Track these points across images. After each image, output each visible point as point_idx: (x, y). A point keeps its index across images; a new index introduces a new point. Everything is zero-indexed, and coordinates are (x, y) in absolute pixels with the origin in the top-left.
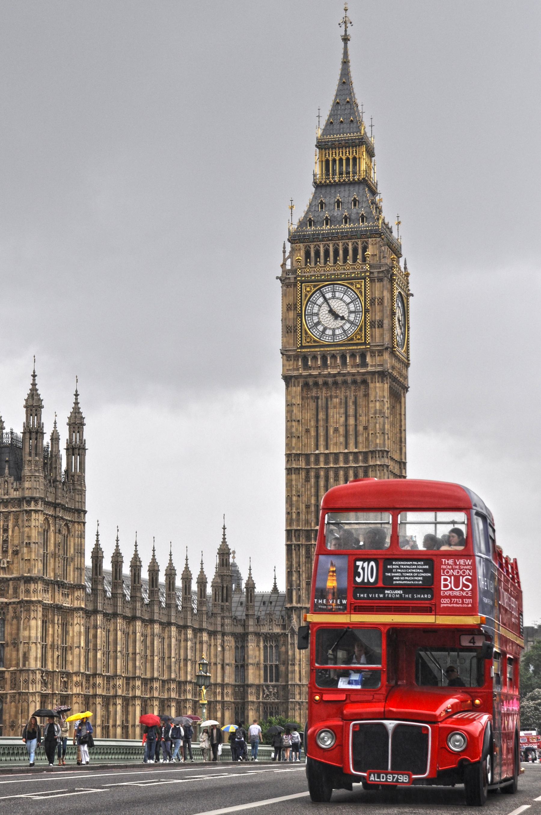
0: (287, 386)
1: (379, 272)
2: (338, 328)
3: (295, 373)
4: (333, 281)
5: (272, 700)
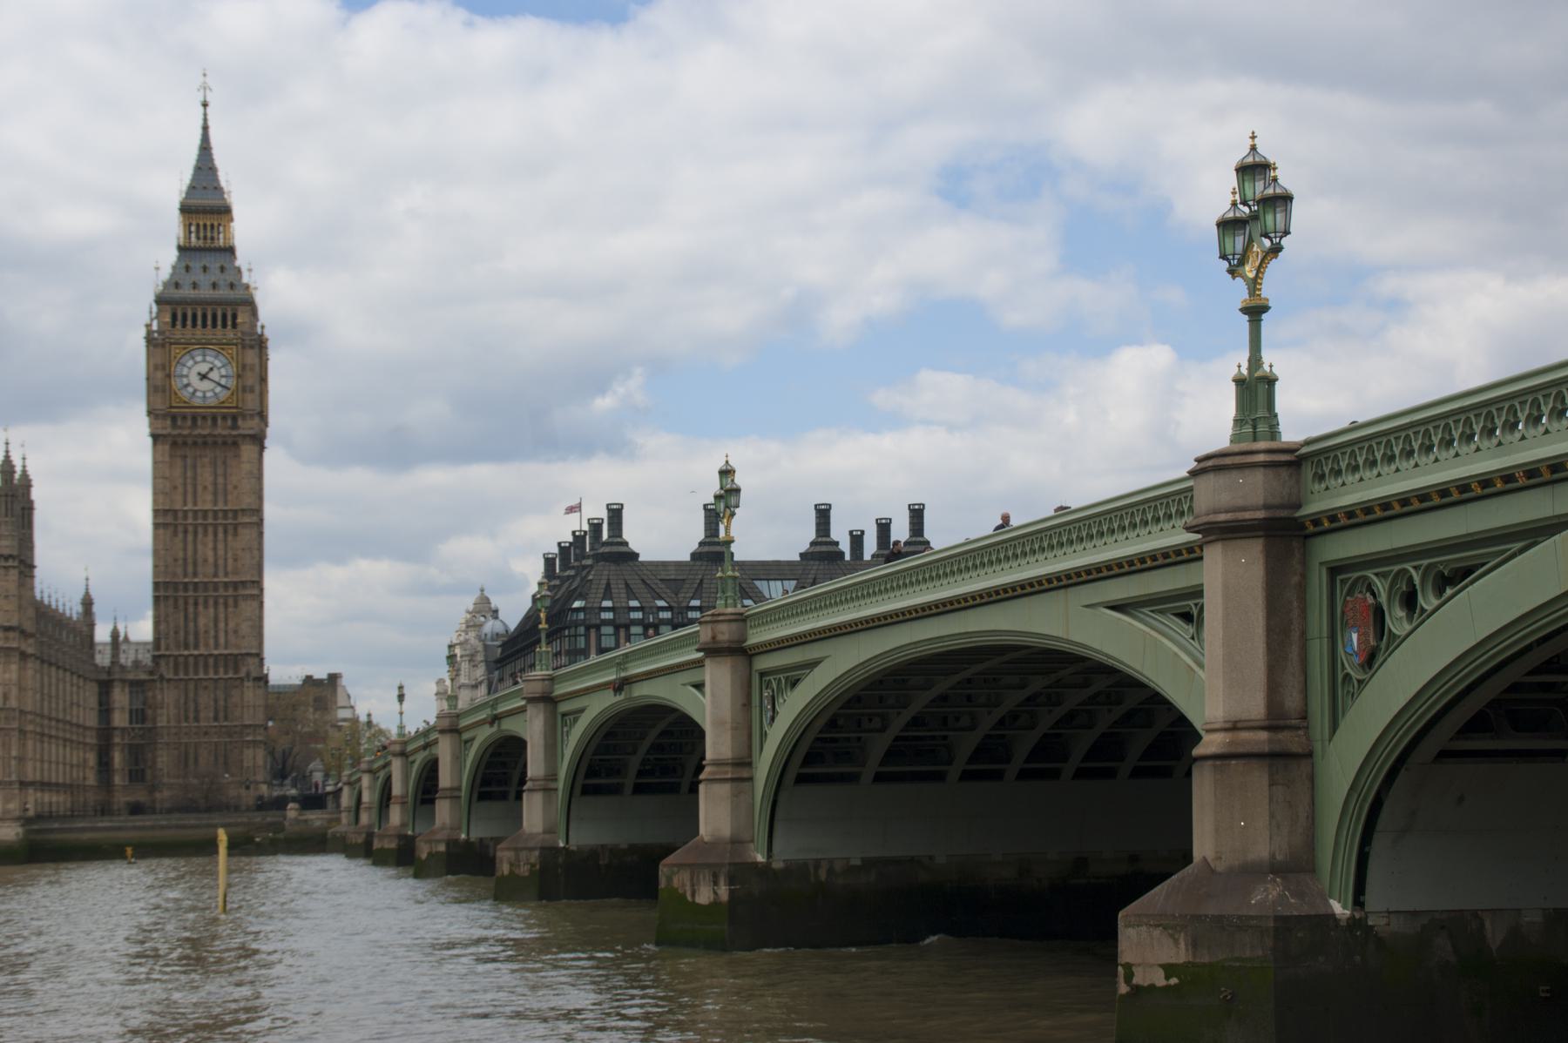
1: (251, 340)
2: (208, 391)
3: (164, 432)
4: (204, 345)
5: (136, 742)
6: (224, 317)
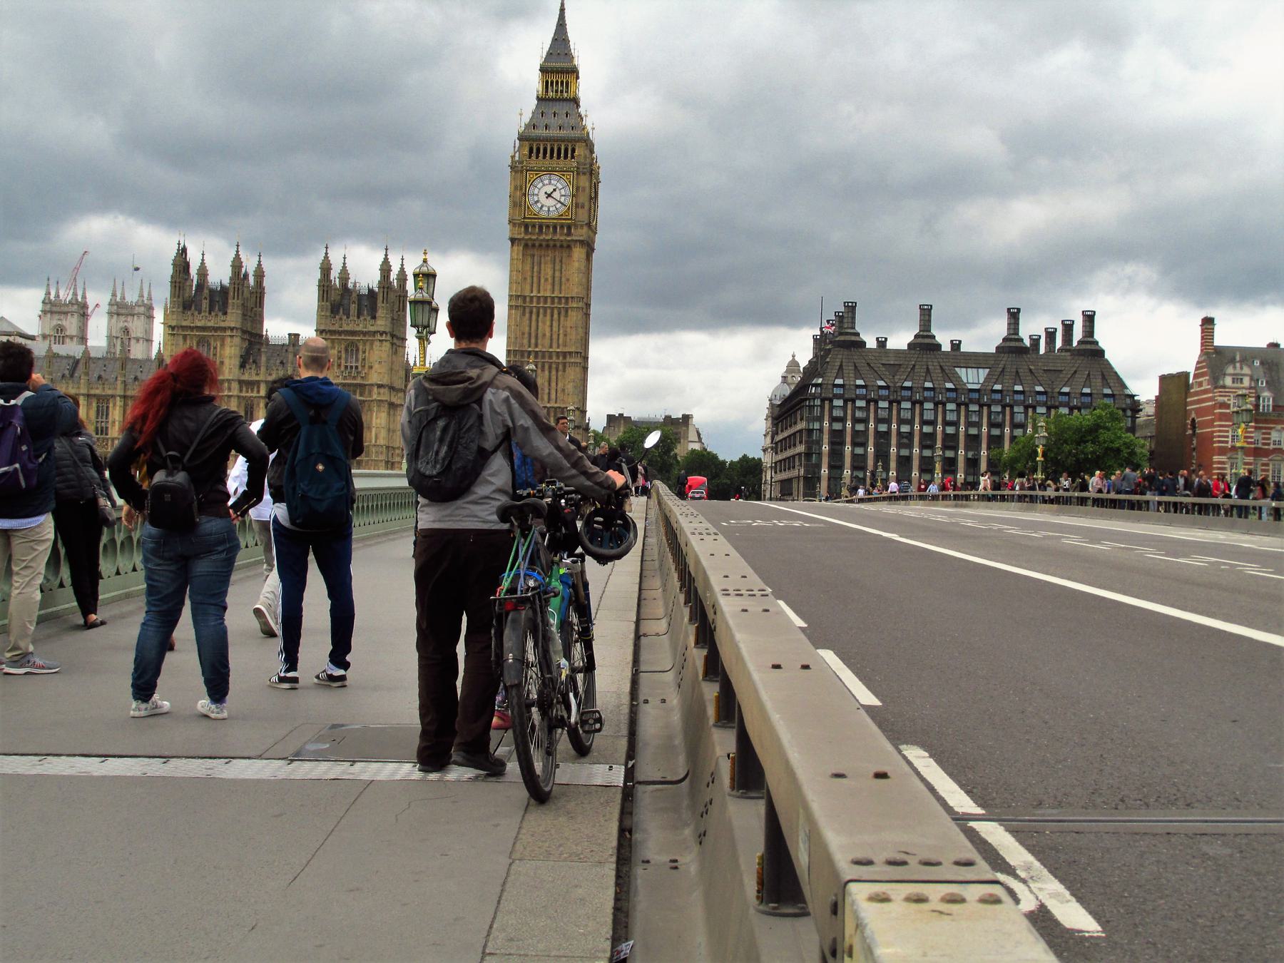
0: (512, 245)
4: (550, 171)
6: (566, 151)
